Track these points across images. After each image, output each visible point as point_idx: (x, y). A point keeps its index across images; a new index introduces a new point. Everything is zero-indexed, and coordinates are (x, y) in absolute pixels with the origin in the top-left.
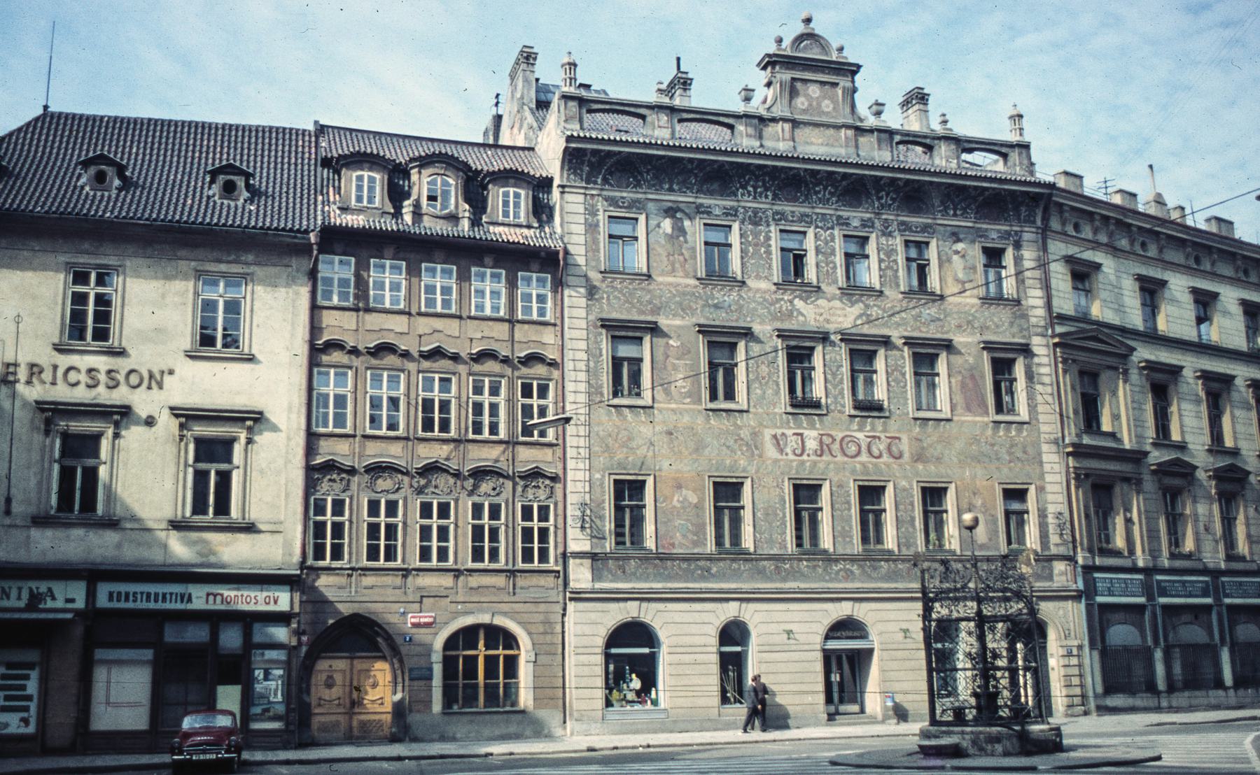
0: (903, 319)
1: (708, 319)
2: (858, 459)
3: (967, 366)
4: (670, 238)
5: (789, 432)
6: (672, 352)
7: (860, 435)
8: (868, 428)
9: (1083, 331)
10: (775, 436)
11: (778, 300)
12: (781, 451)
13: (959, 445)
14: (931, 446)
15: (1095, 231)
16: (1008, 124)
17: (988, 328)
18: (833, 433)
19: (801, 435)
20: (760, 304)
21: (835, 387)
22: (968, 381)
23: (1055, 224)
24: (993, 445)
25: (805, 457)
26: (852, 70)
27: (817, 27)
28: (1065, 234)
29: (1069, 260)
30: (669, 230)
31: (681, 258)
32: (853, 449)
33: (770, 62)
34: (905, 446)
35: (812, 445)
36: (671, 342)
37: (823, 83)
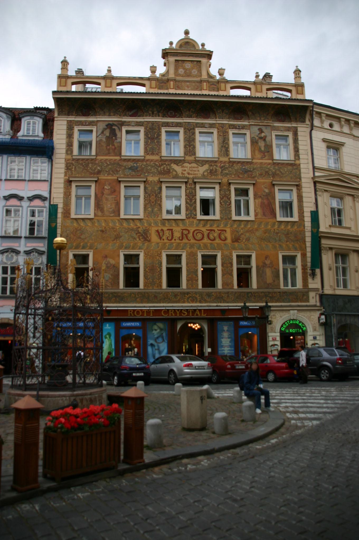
0: (230, 171)
1: (125, 175)
2: (203, 241)
3: (264, 194)
4: (108, 138)
5: (165, 229)
6: (106, 192)
7: (204, 229)
8: (208, 226)
9: (330, 175)
10: (157, 231)
11: (162, 165)
12: (160, 238)
13: (258, 234)
14: (242, 234)
15: (341, 127)
16: (293, 76)
17: (278, 175)
18: (189, 229)
19: (172, 230)
20: (152, 167)
21: (191, 205)
22: (265, 201)
23: (317, 122)
24: (277, 233)
25: (173, 241)
26: (209, 55)
27: (191, 36)
28: (322, 128)
29: (324, 140)
30: (108, 135)
31: (113, 147)
32: (200, 236)
33: (165, 54)
34: (228, 235)
35: (177, 235)
36: (106, 187)
37: (192, 61)
